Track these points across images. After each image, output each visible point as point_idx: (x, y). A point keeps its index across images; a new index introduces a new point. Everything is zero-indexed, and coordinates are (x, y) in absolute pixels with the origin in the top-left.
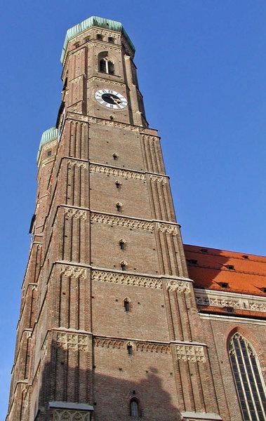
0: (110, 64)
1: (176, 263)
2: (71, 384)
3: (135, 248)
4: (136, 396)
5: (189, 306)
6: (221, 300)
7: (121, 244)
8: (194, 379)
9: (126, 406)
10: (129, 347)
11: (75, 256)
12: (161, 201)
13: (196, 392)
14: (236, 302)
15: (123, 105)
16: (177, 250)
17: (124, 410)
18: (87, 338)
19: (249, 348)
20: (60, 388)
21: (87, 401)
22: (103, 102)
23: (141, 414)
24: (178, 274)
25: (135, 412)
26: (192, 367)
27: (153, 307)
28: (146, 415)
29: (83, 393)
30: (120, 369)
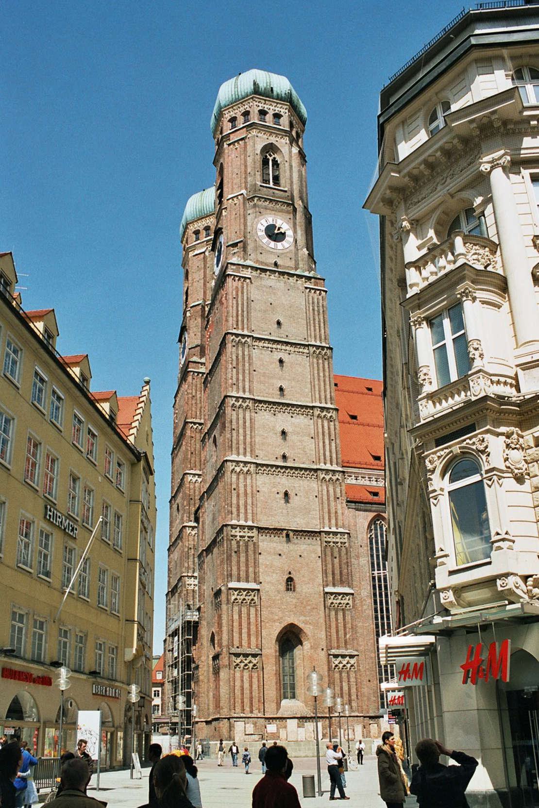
0: (275, 162)
2: (243, 568)
5: (339, 495)
7: (284, 433)
8: (336, 561)
9: (284, 584)
10: (288, 536)
11: (241, 451)
12: (322, 379)
13: (337, 572)
15: (288, 242)
16: (333, 437)
17: (283, 587)
18: (255, 530)
24: (332, 465)
27: (309, 498)
28: (298, 589)
29: (251, 575)
30: (280, 555)
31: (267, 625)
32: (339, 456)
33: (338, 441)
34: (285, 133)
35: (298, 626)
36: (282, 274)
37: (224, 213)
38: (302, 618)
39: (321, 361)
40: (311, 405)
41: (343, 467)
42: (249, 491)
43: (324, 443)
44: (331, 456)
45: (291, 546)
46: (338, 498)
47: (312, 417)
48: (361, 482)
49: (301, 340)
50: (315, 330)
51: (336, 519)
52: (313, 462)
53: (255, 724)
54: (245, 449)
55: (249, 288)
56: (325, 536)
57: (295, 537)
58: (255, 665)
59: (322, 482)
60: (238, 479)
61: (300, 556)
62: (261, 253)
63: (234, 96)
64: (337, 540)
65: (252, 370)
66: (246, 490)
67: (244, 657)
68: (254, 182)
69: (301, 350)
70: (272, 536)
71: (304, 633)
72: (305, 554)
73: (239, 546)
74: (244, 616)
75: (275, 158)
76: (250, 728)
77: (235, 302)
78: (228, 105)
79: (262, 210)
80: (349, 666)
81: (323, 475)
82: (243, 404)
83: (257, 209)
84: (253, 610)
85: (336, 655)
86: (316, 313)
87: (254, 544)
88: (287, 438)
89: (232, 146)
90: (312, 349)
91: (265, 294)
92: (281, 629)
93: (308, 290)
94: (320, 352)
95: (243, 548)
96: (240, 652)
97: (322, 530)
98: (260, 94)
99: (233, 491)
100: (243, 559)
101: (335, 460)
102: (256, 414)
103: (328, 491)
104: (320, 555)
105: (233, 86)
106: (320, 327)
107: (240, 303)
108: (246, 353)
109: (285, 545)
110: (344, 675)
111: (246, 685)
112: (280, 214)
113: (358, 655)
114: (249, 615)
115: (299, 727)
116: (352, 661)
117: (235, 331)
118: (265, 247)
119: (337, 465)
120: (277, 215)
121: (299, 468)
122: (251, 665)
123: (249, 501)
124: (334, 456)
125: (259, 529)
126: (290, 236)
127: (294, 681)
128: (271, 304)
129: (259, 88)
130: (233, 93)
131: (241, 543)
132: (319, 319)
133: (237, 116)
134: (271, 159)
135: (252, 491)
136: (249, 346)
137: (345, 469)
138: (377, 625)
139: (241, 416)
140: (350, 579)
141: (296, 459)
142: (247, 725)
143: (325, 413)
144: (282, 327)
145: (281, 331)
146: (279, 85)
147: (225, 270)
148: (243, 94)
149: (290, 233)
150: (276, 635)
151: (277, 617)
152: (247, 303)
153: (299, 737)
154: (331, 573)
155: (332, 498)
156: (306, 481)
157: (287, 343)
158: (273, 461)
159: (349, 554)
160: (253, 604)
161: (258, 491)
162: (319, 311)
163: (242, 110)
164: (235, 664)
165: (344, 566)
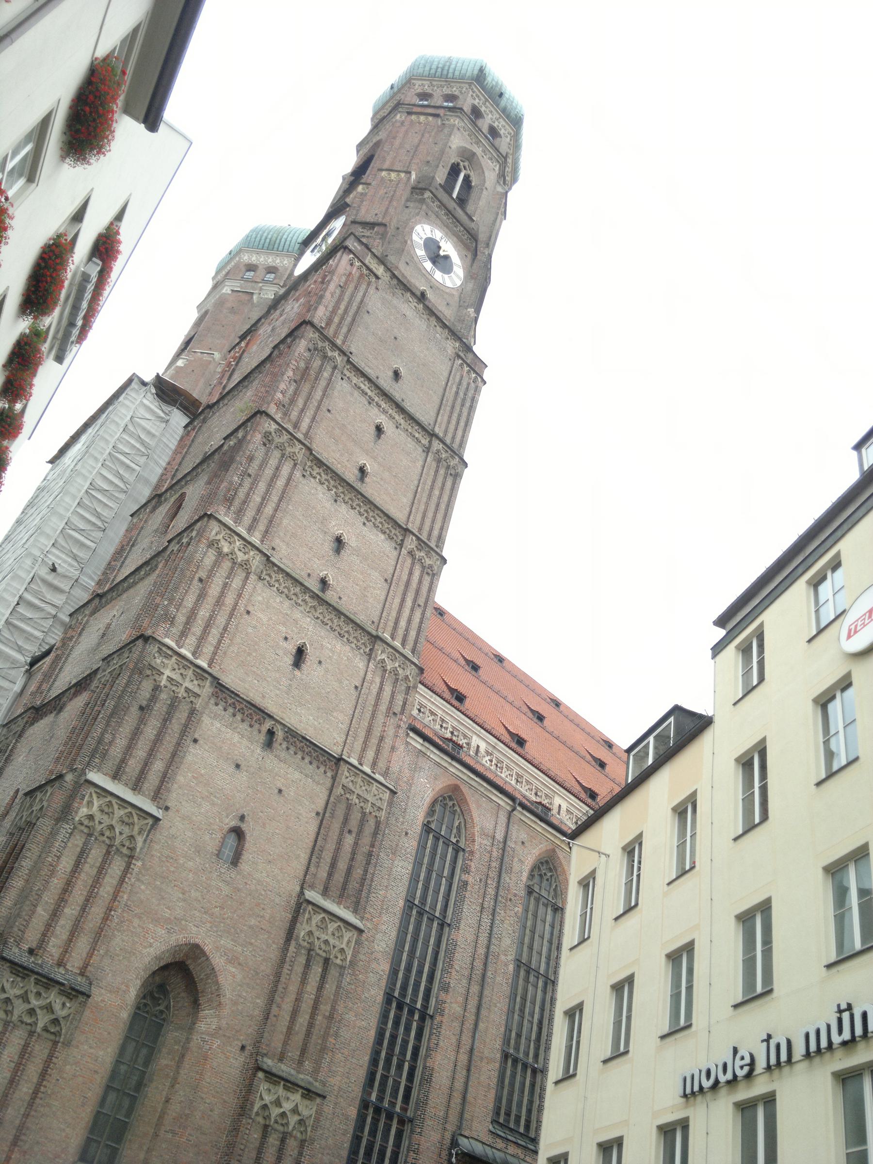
0: (467, 180)
1: (409, 621)
2: (140, 753)
3: (354, 558)
4: (244, 827)
6: (443, 721)
7: (339, 542)
8: (349, 840)
9: (219, 836)
10: (271, 733)
13: (342, 865)
14: (465, 736)
19: (459, 828)
20: (116, 751)
21: (156, 796)
22: (421, 252)
23: (235, 861)
25: (228, 853)
26: (356, 816)
27: (341, 682)
28: (245, 866)
30: (238, 766)
31: (136, 922)
35: (208, 959)
37: (360, 188)
39: (442, 472)
42: (229, 600)
43: (403, 600)
45: (271, 761)
46: (395, 714)
47: (397, 547)
51: (378, 752)
52: (373, 622)
54: (255, 520)
56: (346, 773)
57: (284, 745)
58: (56, 1021)
59: (376, 667)
60: (216, 564)
61: (280, 791)
62: (407, 263)
64: (369, 797)
66: (222, 594)
67: (37, 982)
69: (417, 435)
70: (239, 717)
71: (217, 983)
72: (290, 793)
73: (153, 698)
74: (89, 870)
77: (338, 291)
79: (430, 213)
80: (293, 1119)
81: (384, 656)
82: (286, 445)
83: (424, 207)
84: (117, 866)
86: (459, 401)
87: (192, 712)
88: (342, 552)
90: (436, 445)
91: (392, 317)
92: (163, 948)
95: (160, 708)
96: (32, 966)
99: (196, 582)
100: (150, 731)
101: (412, 643)
102: (301, 479)
103: (381, 689)
104: (321, 812)
108: (326, 375)
109: (259, 751)
110: (273, 1140)
112: (455, 239)
114: (101, 870)
116: (307, 1109)
122: (43, 1020)
123: (221, 620)
125: (220, 687)
126: (458, 276)
127: (128, 1114)
128: (395, 338)
129: (485, 79)
131: (163, 696)
132: (461, 411)
133: (434, 94)
135: (236, 604)
136: (335, 367)
138: (380, 1034)
139: (273, 462)
140: (364, 894)
141: (344, 599)
143: (422, 554)
144: (399, 382)
145: (396, 386)
148: (457, 73)
150: (147, 960)
151: (167, 914)
152: (359, 308)
154: (329, 860)
155: (383, 708)
156: (347, 648)
159: (380, 837)
160: (125, 851)
161: (248, 612)
162: (464, 400)
163: (447, 91)
164: (4, 996)
165: (360, 858)
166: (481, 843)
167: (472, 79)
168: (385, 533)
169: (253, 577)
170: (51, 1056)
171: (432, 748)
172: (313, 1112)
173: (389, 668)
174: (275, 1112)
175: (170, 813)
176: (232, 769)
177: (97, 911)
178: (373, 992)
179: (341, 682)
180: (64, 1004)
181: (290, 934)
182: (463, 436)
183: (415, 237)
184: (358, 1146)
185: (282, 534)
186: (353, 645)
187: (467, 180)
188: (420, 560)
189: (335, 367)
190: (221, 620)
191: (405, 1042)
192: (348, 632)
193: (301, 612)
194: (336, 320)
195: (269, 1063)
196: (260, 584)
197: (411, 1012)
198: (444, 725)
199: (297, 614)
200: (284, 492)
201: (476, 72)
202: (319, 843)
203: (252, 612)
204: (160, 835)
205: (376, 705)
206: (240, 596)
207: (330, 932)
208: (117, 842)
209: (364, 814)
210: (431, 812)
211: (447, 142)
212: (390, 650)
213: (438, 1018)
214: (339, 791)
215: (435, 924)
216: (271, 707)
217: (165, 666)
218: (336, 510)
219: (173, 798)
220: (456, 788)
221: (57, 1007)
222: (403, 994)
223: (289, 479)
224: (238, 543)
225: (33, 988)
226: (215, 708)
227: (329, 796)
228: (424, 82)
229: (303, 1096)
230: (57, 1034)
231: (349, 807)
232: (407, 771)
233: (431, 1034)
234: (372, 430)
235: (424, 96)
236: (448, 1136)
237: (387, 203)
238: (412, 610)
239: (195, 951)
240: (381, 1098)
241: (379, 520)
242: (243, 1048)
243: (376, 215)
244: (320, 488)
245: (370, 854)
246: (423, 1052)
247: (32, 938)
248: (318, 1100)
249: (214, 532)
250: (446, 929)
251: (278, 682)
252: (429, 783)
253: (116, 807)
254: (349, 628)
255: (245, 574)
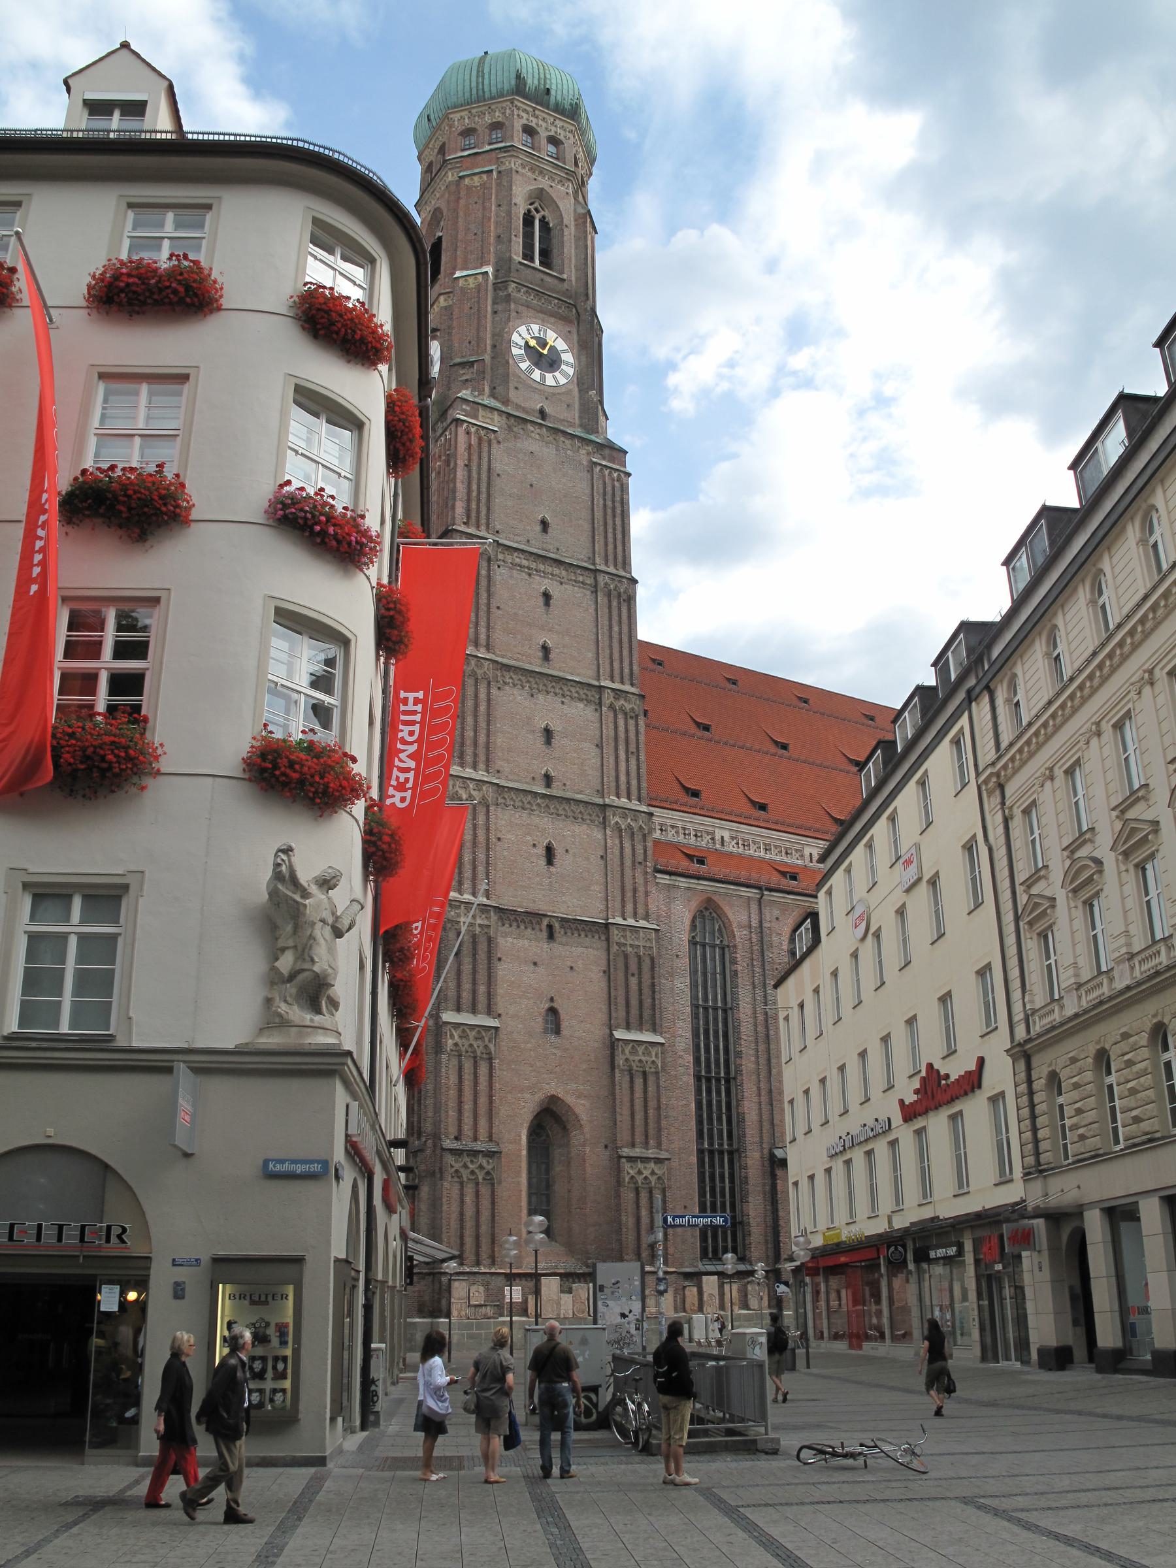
0: (544, 223)
2: (467, 986)
3: (566, 741)
4: (555, 1005)
6: (684, 829)
7: (548, 733)
8: (633, 981)
9: (540, 1019)
10: (550, 927)
11: (469, 758)
12: (616, 636)
13: (634, 1002)
14: (708, 833)
15: (564, 374)
16: (632, 748)
17: (538, 1024)
21: (489, 1012)
23: (557, 1031)
24: (629, 798)
27: (588, 859)
28: (565, 1031)
30: (535, 964)
31: (509, 1096)
32: (644, 785)
33: (642, 757)
34: (567, 174)
35: (563, 1101)
36: (556, 431)
38: (572, 1086)
40: (597, 683)
41: (649, 805)
42: (481, 837)
43: (617, 757)
44: (628, 783)
45: (557, 948)
46: (640, 863)
48: (670, 836)
49: (582, 560)
50: (606, 544)
53: (486, 1285)
54: (475, 755)
55: (494, 451)
56: (616, 932)
58: (488, 1173)
61: (571, 968)
63: (474, 91)
65: (494, 603)
67: (468, 1155)
68: (508, 255)
70: (522, 927)
71: (575, 1114)
72: (579, 965)
75: (544, 217)
76: (478, 1295)
78: (462, 106)
79: (520, 308)
84: (483, 1068)
85: (632, 1157)
86: (609, 511)
89: (467, 181)
91: (522, 465)
93: (599, 468)
94: (616, 586)
96: (461, 1147)
97: (610, 921)
98: (526, 97)
103: (622, 848)
105: (474, 73)
106: (615, 539)
107: (475, 475)
109: (546, 945)
110: (644, 1195)
111: (469, 1211)
112: (553, 320)
113: (669, 1159)
115: (562, 1292)
117: (463, 528)
118: (523, 376)
119: (639, 800)
120: (548, 322)
121: (573, 800)
123: (481, 856)
124: (634, 783)
126: (568, 364)
127: (548, 1205)
128: (531, 485)
129: (525, 85)
130: (474, 84)
133: (478, 127)
134: (538, 217)
136: (489, 560)
137: (652, 809)
140: (657, 1016)
141: (568, 783)
142: (473, 1289)
143: (622, 702)
144: (550, 530)
145: (547, 538)
146: (560, 86)
147: (446, 411)
148: (494, 90)
149: (568, 357)
151: (526, 1083)
152: (489, 478)
153: (562, 1312)
155: (628, 862)
156: (585, 826)
157: (558, 562)
158: (527, 783)
160: (485, 1056)
161: (499, 839)
162: (614, 509)
163: (488, 119)
164: (453, 1170)
165: (646, 991)
166: (740, 934)
167: (513, 94)
168: (581, 700)
169: (492, 808)
170: (493, 1192)
171: (679, 879)
172: (665, 1169)
173: (623, 827)
174: (640, 1179)
175: (503, 1017)
176: (532, 968)
177: (483, 1100)
178: (684, 1079)
179: (588, 859)
180: (488, 1162)
181: (613, 1066)
182: (624, 551)
183: (515, 351)
184: (704, 1178)
185: (500, 754)
186: (588, 821)
187: (543, 221)
188: (621, 709)
189: (489, 560)
190: (481, 856)
191: (719, 1102)
192: (581, 812)
193: (539, 816)
194: (474, 506)
195: (626, 1151)
196: (499, 810)
197: (718, 1080)
198: (687, 832)
199: (536, 820)
200: (488, 715)
201: (513, 82)
202: (612, 994)
203: (502, 837)
204: (503, 1035)
205: (622, 864)
206: (488, 829)
207: (640, 1053)
208: (479, 1053)
209: (639, 957)
210: (693, 927)
211: (511, 200)
212: (620, 810)
213: (739, 1078)
214: (615, 948)
215: (720, 1012)
216: (542, 907)
217: (459, 915)
218: (535, 704)
219: (501, 1005)
220: (709, 900)
221: (485, 1164)
222: (708, 1070)
223: (489, 700)
224: (471, 786)
225: (467, 1159)
226: (503, 929)
227: (609, 955)
228: (463, 114)
229: (655, 1163)
230: (492, 1179)
231: (626, 957)
232: (663, 907)
233: (737, 1090)
234: (541, 600)
235: (468, 132)
236: (766, 1151)
237: (476, 321)
238: (627, 761)
239: (553, 1099)
240: (711, 1144)
241: (573, 690)
242: (606, 1147)
243: (470, 342)
244: (516, 692)
245: (653, 985)
246: (734, 1103)
247: (453, 1130)
248: (666, 1162)
249: (451, 787)
250: (730, 1012)
251: (541, 884)
252: (684, 907)
253: (468, 1031)
254: (581, 808)
255: (485, 809)
